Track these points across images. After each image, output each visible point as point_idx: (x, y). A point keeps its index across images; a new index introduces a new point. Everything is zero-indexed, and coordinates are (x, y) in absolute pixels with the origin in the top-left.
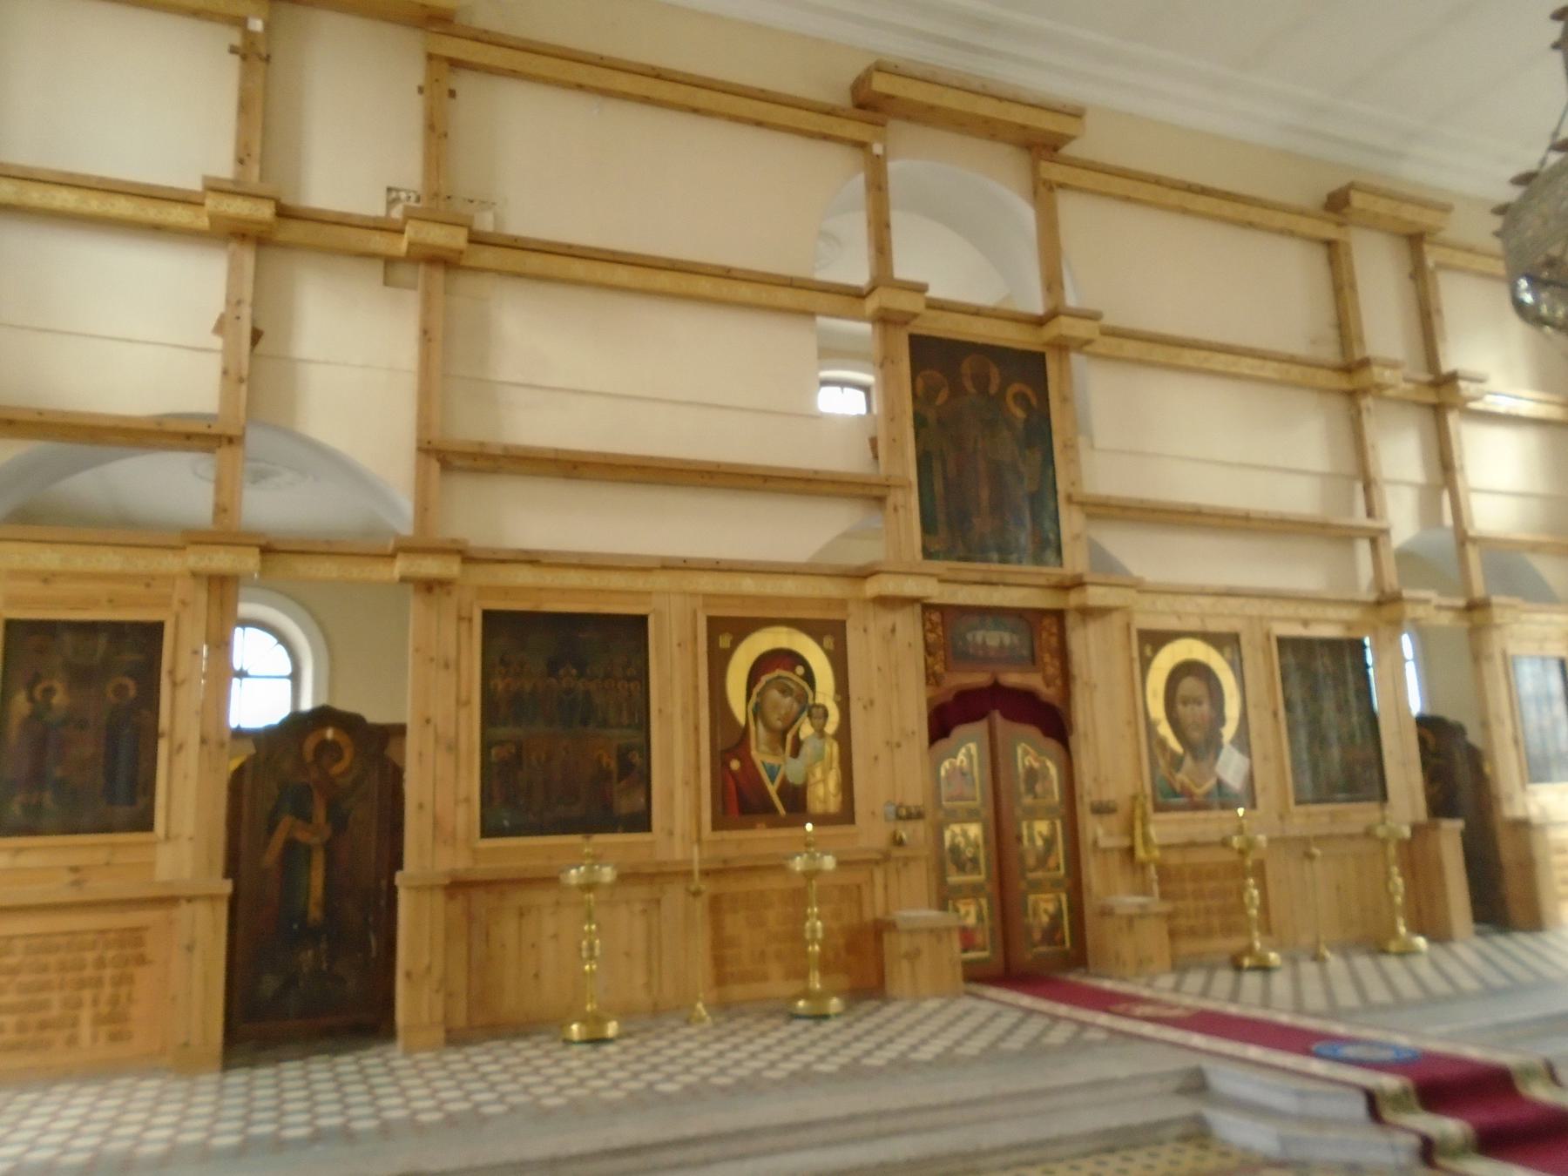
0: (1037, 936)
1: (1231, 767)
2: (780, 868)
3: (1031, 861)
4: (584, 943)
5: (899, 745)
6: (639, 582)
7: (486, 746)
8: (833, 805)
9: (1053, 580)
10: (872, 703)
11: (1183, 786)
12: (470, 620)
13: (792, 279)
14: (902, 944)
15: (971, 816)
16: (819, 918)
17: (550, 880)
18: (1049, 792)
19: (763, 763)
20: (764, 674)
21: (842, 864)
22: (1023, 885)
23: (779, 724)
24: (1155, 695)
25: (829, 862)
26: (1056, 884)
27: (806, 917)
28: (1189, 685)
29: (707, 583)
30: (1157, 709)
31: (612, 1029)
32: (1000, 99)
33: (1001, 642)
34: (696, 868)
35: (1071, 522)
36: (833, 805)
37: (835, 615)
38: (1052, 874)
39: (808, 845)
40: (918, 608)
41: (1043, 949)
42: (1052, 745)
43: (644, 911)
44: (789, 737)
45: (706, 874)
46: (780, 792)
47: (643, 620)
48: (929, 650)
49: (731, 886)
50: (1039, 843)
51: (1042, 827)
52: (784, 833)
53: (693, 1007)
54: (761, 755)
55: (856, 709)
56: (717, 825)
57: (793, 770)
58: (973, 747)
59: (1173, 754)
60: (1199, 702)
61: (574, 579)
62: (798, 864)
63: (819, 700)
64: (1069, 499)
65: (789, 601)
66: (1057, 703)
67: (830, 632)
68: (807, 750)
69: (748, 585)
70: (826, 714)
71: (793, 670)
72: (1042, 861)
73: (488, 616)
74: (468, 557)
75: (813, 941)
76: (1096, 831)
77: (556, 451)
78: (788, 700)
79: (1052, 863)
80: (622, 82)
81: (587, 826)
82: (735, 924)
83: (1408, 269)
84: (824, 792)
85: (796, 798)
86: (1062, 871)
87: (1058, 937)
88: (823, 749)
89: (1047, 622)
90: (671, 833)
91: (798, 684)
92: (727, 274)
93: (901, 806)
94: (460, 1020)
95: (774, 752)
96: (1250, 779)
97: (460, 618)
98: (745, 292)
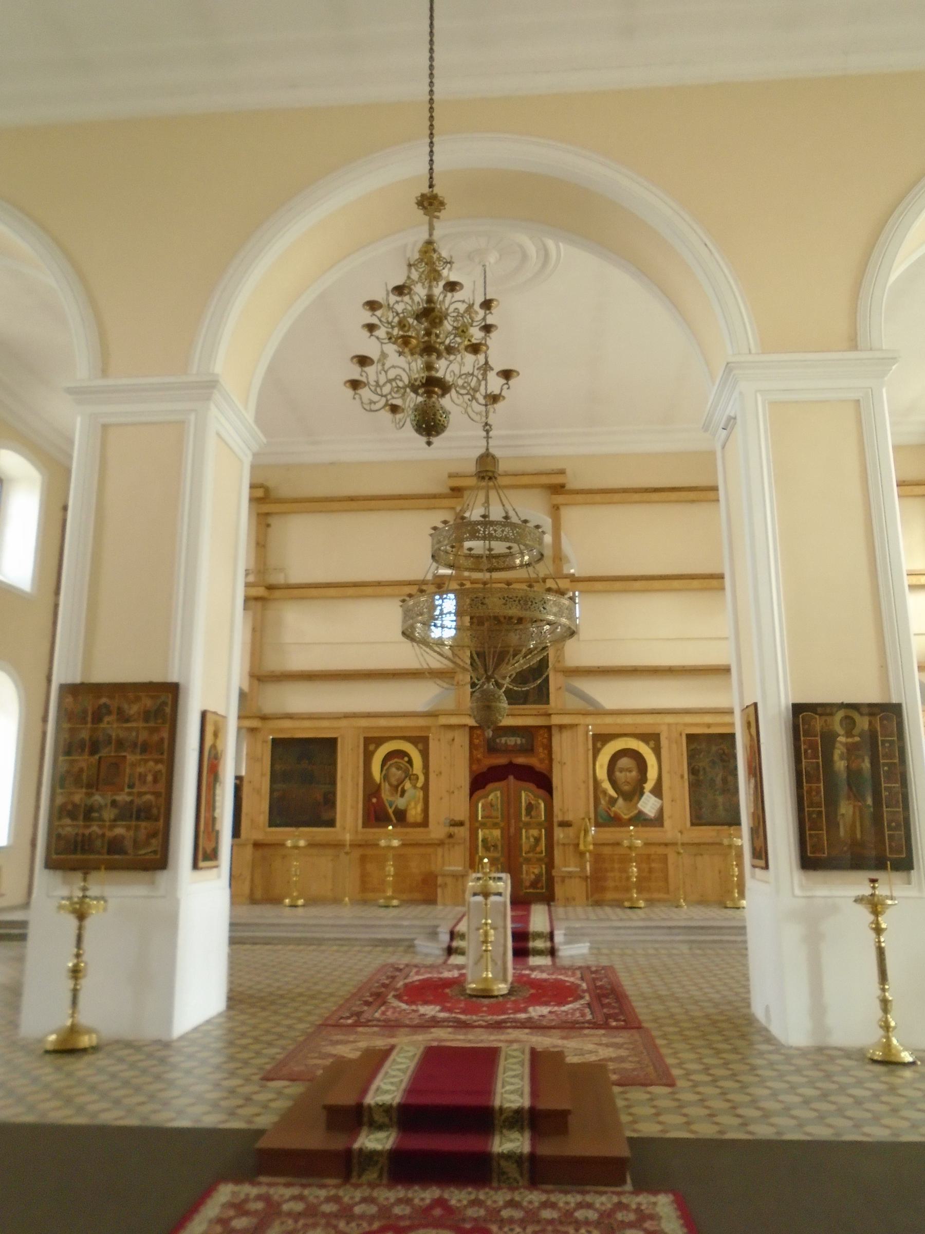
0: (528, 884)
1: (648, 805)
2: (377, 845)
3: (525, 848)
5: (453, 792)
6: (336, 724)
7: (272, 791)
8: (419, 819)
9: (541, 712)
10: (441, 773)
11: (616, 813)
14: (440, 880)
15: (495, 825)
17: (282, 845)
18: (539, 815)
19: (387, 800)
22: (521, 860)
23: (395, 783)
24: (601, 766)
26: (540, 860)
28: (624, 762)
29: (364, 723)
30: (602, 773)
32: (516, 475)
33: (516, 742)
35: (555, 681)
36: (419, 819)
37: (423, 734)
38: (538, 856)
40: (467, 729)
41: (531, 891)
42: (541, 792)
43: (332, 860)
44: (400, 789)
45: (354, 845)
46: (394, 812)
48: (472, 747)
49: (369, 852)
50: (532, 840)
51: (535, 832)
54: (386, 794)
55: (432, 776)
56: (363, 827)
57: (401, 803)
58: (498, 793)
59: (611, 797)
60: (630, 771)
61: (307, 724)
62: (383, 843)
63: (414, 772)
64: (556, 670)
65: (401, 728)
66: (545, 772)
67: (421, 742)
68: (406, 795)
69: (383, 722)
70: (417, 778)
71: (403, 758)
72: (533, 849)
74: (264, 718)
75: (389, 875)
76: (559, 834)
77: (302, 671)
78: (400, 772)
79: (538, 849)
80: (336, 505)
82: (370, 867)
84: (414, 813)
85: (401, 816)
86: (544, 854)
87: (540, 885)
89: (541, 732)
90: (344, 828)
91: (405, 766)
92: (379, 584)
93: (453, 820)
94: (258, 894)
95: (392, 795)
96: (661, 811)
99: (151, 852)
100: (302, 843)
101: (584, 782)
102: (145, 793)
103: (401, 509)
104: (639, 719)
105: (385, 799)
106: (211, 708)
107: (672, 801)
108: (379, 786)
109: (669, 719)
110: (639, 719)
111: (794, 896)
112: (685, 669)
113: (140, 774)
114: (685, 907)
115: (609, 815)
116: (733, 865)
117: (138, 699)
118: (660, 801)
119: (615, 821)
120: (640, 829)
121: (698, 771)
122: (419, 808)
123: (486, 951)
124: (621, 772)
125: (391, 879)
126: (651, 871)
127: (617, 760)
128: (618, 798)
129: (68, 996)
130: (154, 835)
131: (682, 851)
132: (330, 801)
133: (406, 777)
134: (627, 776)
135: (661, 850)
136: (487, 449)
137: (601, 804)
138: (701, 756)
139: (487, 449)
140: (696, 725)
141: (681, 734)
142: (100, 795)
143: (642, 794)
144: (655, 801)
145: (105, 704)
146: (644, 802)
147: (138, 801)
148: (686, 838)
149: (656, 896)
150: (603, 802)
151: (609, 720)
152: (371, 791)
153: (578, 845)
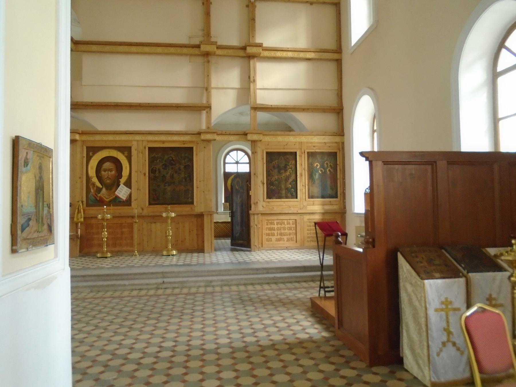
1: (122, 192)
11: (100, 197)
24: (92, 168)
28: (107, 165)
30: (92, 173)
59: (97, 187)
60: (111, 171)
96: (130, 195)
101: (80, 178)
104: (118, 138)
107: (138, 189)
109: (138, 137)
110: (118, 138)
112: (149, 105)
114: (138, 256)
115: (97, 200)
116: (169, 229)
118: (130, 190)
119: (100, 202)
120: (112, 207)
121: (156, 171)
124: (105, 171)
126: (122, 233)
127: (103, 163)
128: (102, 188)
131: (137, 221)
134: (109, 173)
135: (129, 221)
137: (91, 191)
138: (158, 161)
140: (155, 141)
141: (145, 148)
143: (118, 185)
144: (127, 190)
146: (119, 190)
148: (145, 212)
149: (125, 248)
150: (92, 191)
151: (98, 138)
153: (74, 217)
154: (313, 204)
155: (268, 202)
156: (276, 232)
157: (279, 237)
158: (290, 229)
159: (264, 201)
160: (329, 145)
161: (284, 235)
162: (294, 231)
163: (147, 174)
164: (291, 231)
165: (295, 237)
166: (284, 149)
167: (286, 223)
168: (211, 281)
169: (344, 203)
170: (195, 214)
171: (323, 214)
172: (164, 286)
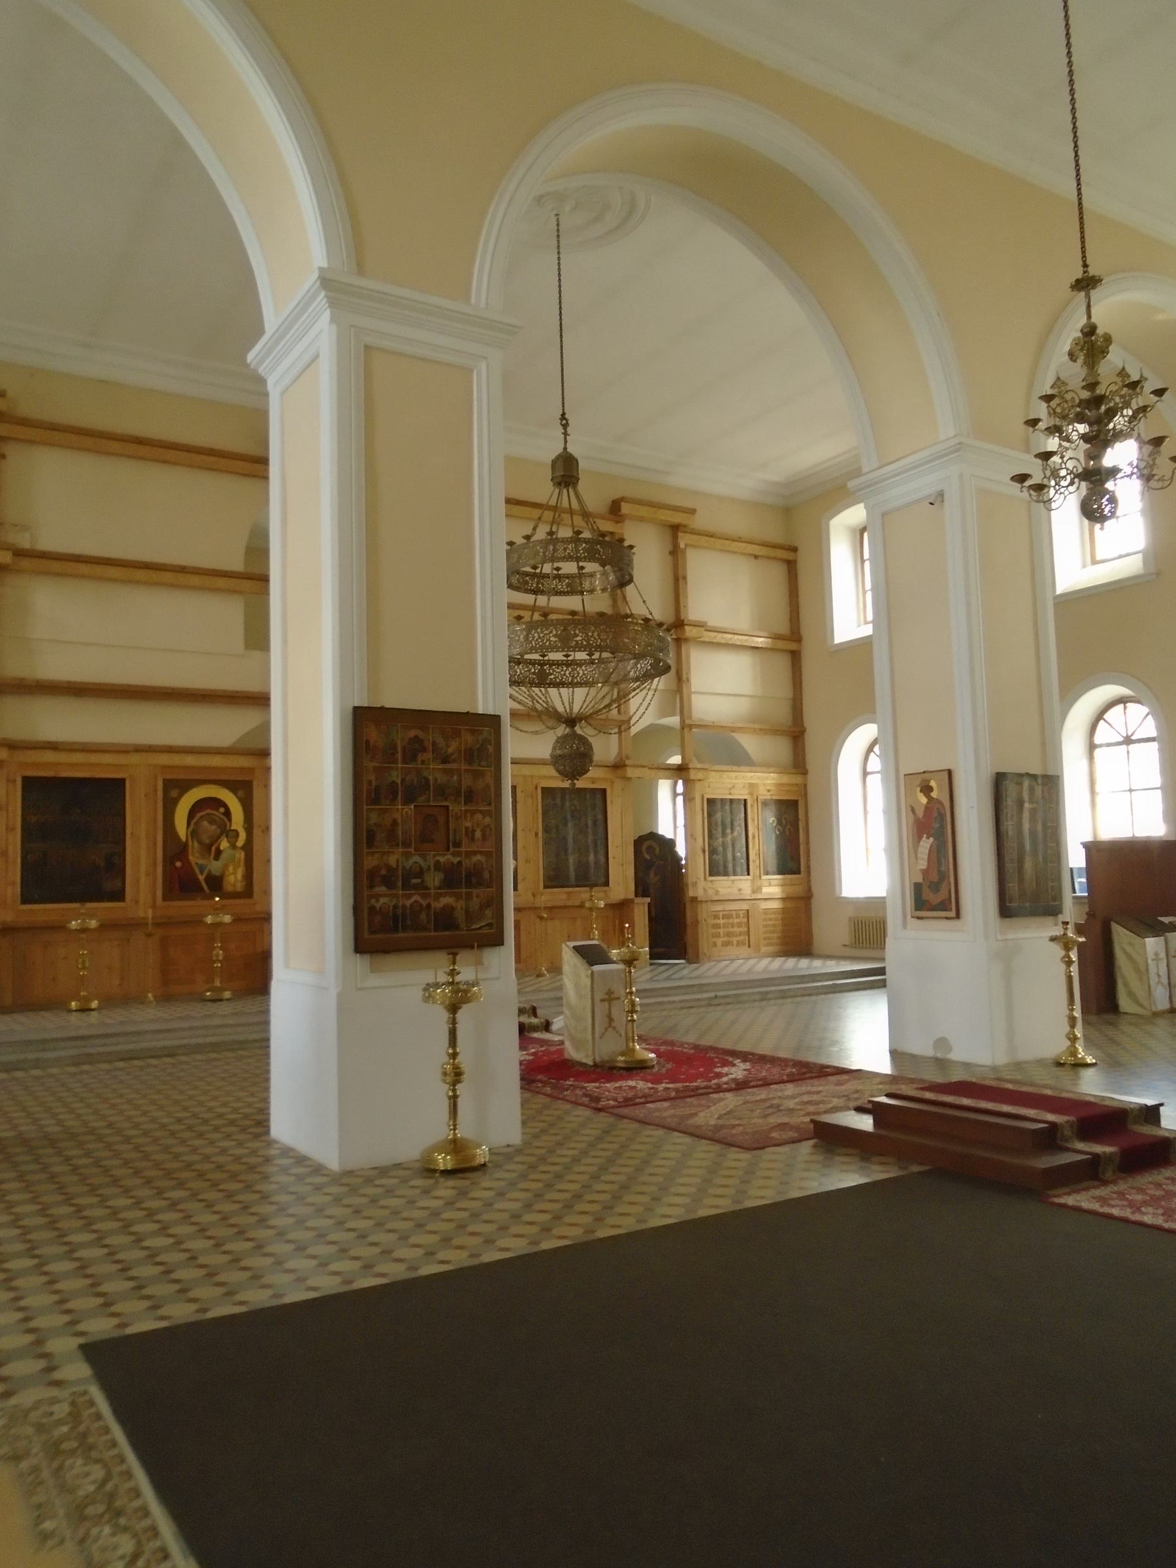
4: (80, 960)
6: (121, 759)
8: (239, 887)
12: (15, 781)
13: (226, 571)
16: (221, 948)
17: (59, 927)
19: (196, 863)
20: (199, 812)
21: (237, 920)
23: (207, 841)
25: (227, 919)
27: (214, 948)
31: (95, 1004)
34: (150, 921)
36: (239, 887)
39: (217, 909)
44: (213, 849)
45: (157, 925)
46: (206, 880)
47: (123, 781)
52: (206, 903)
53: (146, 997)
54: (194, 858)
56: (165, 898)
57: (215, 867)
63: (232, 828)
68: (224, 856)
69: (190, 760)
71: (217, 810)
73: (26, 780)
75: (217, 961)
77: (69, 682)
78: (214, 827)
81: (83, 898)
83: (669, 548)
84: (234, 879)
85: (216, 883)
88: (235, 856)
90: (137, 902)
92: (182, 570)
97: (8, 781)
98: (195, 580)
99: (486, 925)
100: (93, 924)
102: (475, 853)
103: (209, 469)
105: (193, 864)
106: (1011, 767)
107: (526, 861)
108: (186, 845)
111: (997, 940)
113: (467, 828)
117: (457, 733)
122: (240, 872)
123: (633, 1021)
125: (219, 965)
129: (445, 1105)
130: (487, 904)
132: (116, 866)
133: (221, 834)
136: (565, 449)
139: (565, 449)
141: (536, 788)
142: (420, 855)
145: (416, 737)
147: (467, 863)
152: (175, 851)
154: (770, 885)
155: (711, 881)
156: (721, 931)
157: (725, 939)
158: (740, 925)
159: (705, 879)
160: (787, 788)
161: (733, 936)
162: (746, 929)
163: (540, 835)
164: (741, 929)
165: (747, 938)
166: (730, 794)
167: (734, 916)
168: (767, 993)
169: (809, 881)
170: (615, 902)
171: (783, 899)
172: (716, 1001)
